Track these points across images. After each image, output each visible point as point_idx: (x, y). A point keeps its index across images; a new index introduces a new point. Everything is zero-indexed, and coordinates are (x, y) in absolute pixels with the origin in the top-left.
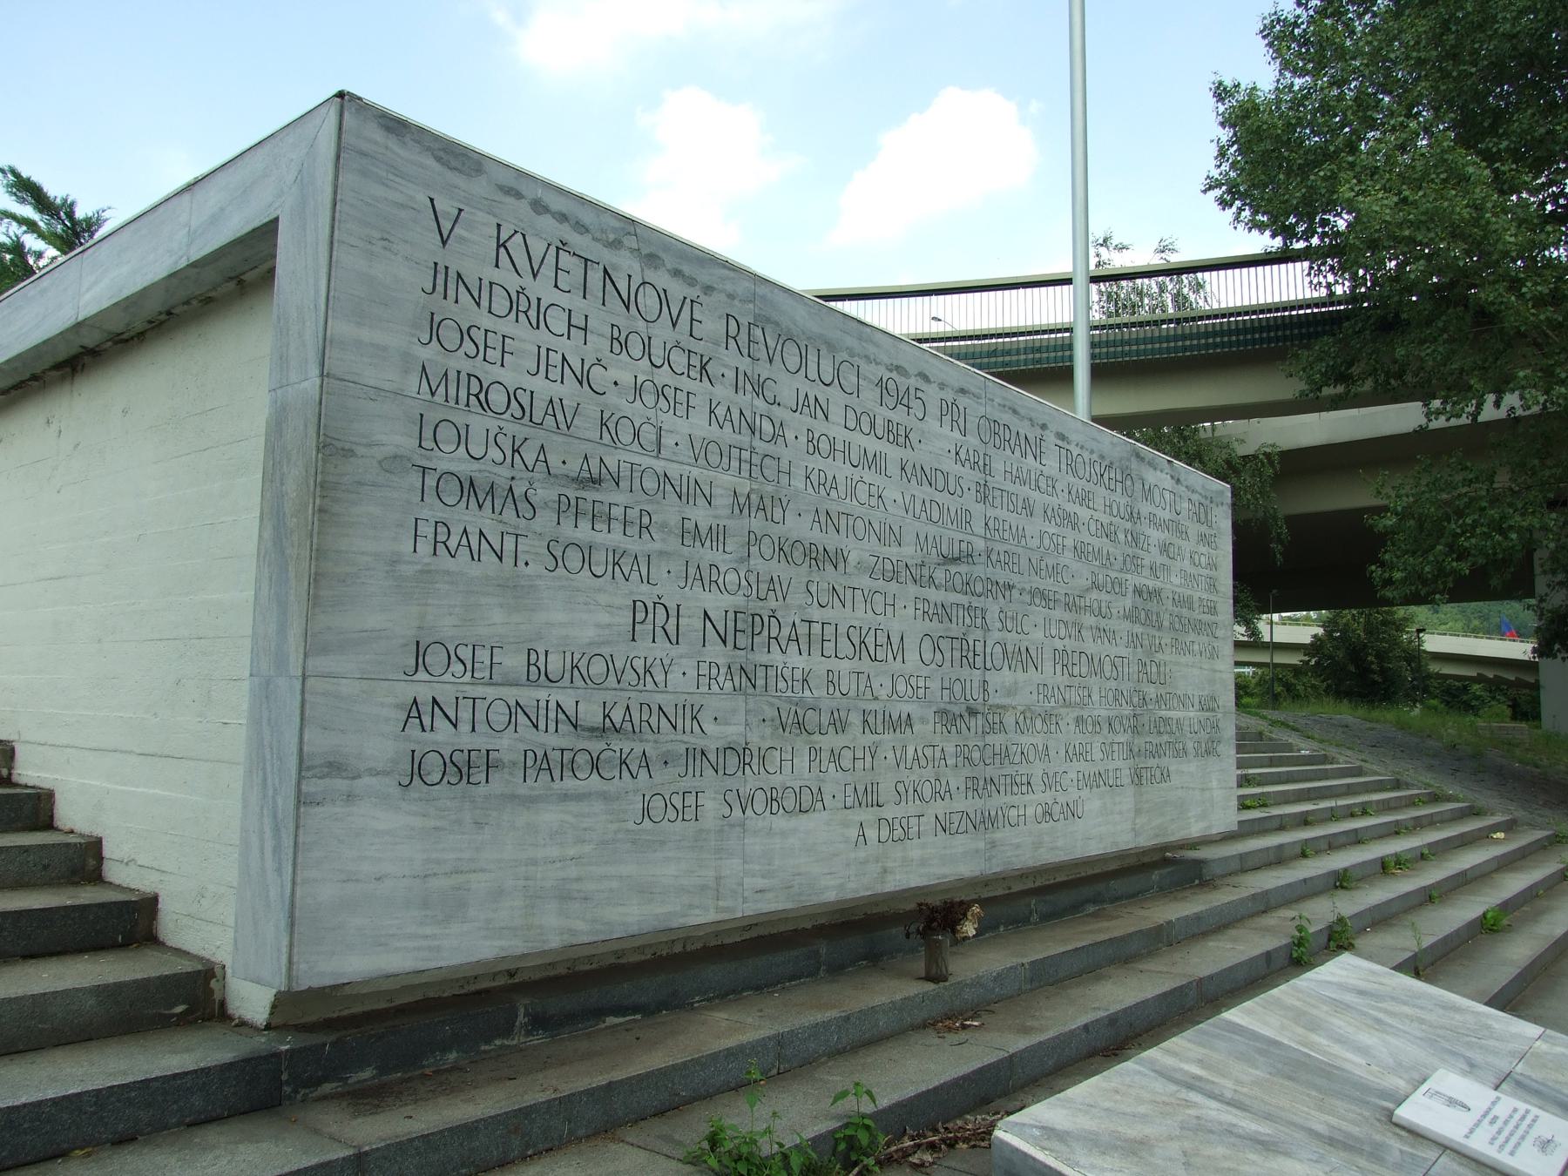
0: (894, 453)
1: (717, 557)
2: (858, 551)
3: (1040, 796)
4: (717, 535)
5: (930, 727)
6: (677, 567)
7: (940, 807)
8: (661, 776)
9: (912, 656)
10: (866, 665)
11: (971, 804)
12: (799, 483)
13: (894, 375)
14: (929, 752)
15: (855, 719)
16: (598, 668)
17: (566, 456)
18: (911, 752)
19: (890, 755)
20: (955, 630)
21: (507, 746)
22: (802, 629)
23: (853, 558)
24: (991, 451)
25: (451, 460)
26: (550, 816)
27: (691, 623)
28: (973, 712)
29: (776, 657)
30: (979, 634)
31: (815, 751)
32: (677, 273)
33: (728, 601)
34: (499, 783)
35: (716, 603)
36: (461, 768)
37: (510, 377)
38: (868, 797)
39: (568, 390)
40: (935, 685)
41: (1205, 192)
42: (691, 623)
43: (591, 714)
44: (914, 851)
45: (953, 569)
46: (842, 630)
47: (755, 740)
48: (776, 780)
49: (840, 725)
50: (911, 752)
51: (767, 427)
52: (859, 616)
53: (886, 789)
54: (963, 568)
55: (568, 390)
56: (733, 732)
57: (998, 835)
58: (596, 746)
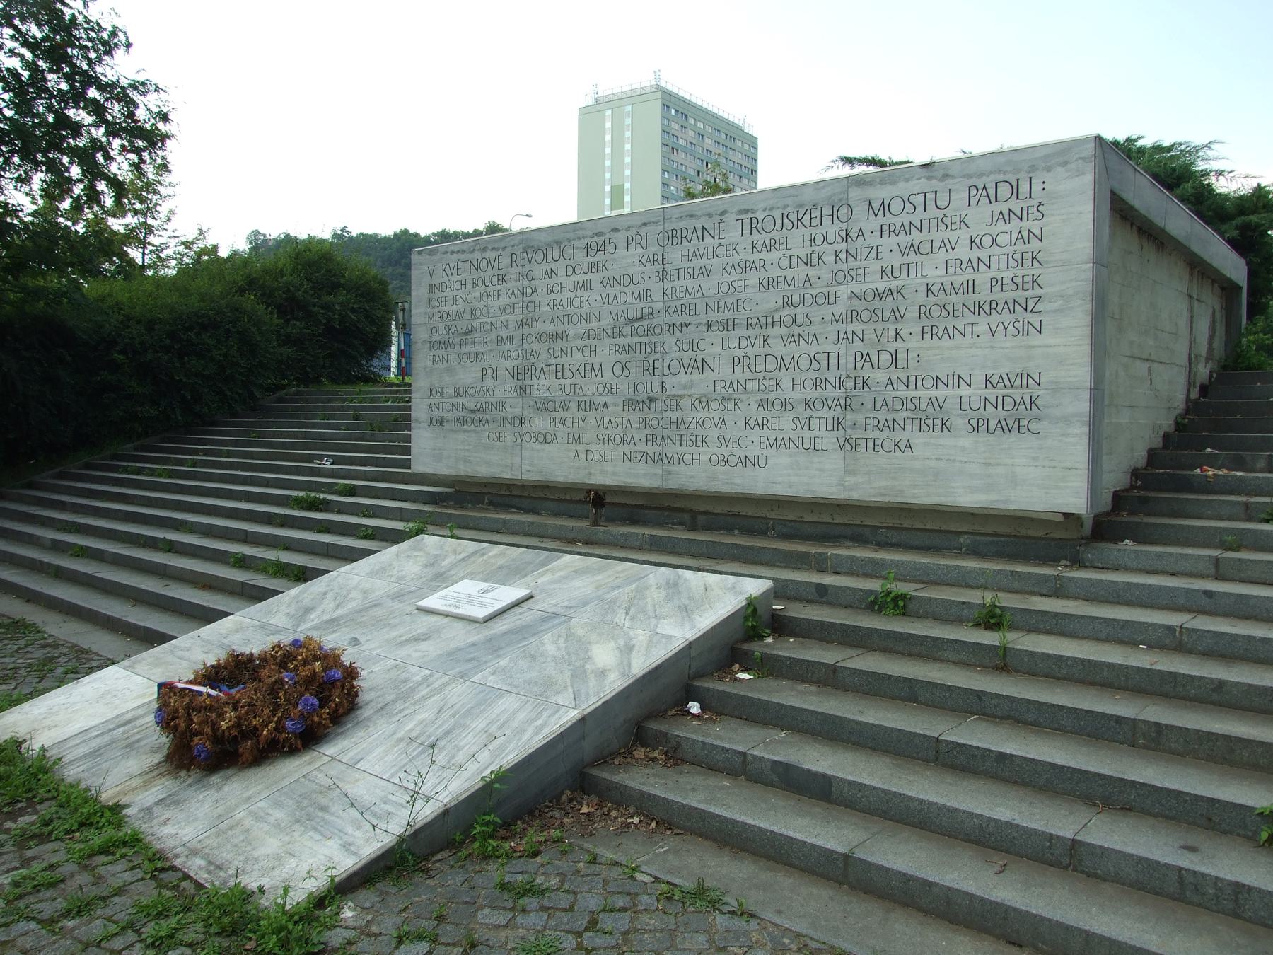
0: (595, 278)
1: (510, 347)
2: (572, 330)
3: (713, 450)
4: (510, 339)
5: (620, 408)
6: (495, 354)
7: (627, 449)
8: (492, 426)
9: (608, 374)
10: (579, 380)
11: (652, 449)
12: (543, 308)
13: (596, 238)
14: (619, 420)
15: (574, 405)
16: (473, 391)
17: (462, 328)
18: (607, 420)
19: (594, 421)
20: (638, 356)
21: (450, 415)
22: (546, 369)
23: (571, 334)
24: (669, 249)
25: (436, 338)
26: (461, 436)
27: (502, 372)
28: (652, 400)
29: (535, 381)
30: (658, 356)
31: (553, 419)
32: (493, 249)
33: (514, 363)
34: (448, 426)
35: (510, 364)
36: (441, 421)
37: (446, 309)
38: (581, 439)
39: (461, 306)
40: (623, 387)
41: (595, 86)
42: (502, 372)
43: (471, 406)
44: (609, 467)
45: (636, 325)
46: (566, 366)
47: (526, 413)
48: (535, 430)
49: (565, 407)
50: (607, 420)
51: (529, 291)
52: (576, 358)
53: (591, 436)
54: (645, 323)
55: (461, 306)
56: (518, 411)
57: (673, 468)
58: (473, 416)
